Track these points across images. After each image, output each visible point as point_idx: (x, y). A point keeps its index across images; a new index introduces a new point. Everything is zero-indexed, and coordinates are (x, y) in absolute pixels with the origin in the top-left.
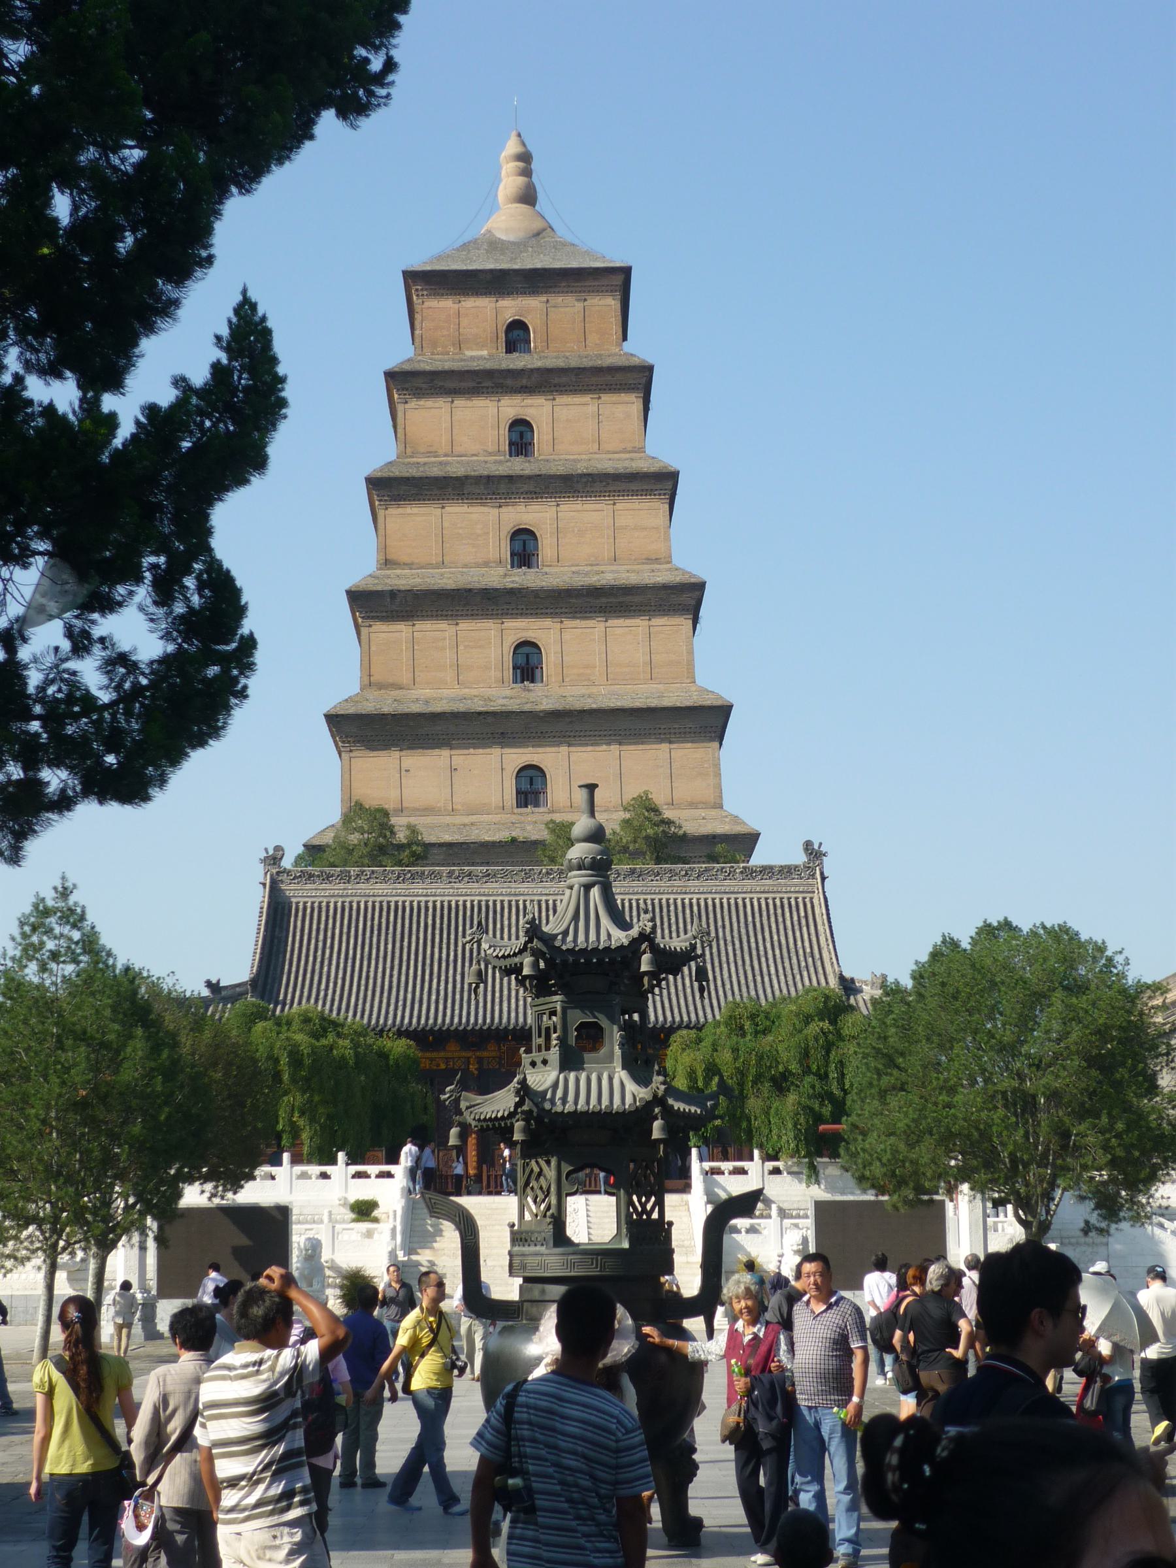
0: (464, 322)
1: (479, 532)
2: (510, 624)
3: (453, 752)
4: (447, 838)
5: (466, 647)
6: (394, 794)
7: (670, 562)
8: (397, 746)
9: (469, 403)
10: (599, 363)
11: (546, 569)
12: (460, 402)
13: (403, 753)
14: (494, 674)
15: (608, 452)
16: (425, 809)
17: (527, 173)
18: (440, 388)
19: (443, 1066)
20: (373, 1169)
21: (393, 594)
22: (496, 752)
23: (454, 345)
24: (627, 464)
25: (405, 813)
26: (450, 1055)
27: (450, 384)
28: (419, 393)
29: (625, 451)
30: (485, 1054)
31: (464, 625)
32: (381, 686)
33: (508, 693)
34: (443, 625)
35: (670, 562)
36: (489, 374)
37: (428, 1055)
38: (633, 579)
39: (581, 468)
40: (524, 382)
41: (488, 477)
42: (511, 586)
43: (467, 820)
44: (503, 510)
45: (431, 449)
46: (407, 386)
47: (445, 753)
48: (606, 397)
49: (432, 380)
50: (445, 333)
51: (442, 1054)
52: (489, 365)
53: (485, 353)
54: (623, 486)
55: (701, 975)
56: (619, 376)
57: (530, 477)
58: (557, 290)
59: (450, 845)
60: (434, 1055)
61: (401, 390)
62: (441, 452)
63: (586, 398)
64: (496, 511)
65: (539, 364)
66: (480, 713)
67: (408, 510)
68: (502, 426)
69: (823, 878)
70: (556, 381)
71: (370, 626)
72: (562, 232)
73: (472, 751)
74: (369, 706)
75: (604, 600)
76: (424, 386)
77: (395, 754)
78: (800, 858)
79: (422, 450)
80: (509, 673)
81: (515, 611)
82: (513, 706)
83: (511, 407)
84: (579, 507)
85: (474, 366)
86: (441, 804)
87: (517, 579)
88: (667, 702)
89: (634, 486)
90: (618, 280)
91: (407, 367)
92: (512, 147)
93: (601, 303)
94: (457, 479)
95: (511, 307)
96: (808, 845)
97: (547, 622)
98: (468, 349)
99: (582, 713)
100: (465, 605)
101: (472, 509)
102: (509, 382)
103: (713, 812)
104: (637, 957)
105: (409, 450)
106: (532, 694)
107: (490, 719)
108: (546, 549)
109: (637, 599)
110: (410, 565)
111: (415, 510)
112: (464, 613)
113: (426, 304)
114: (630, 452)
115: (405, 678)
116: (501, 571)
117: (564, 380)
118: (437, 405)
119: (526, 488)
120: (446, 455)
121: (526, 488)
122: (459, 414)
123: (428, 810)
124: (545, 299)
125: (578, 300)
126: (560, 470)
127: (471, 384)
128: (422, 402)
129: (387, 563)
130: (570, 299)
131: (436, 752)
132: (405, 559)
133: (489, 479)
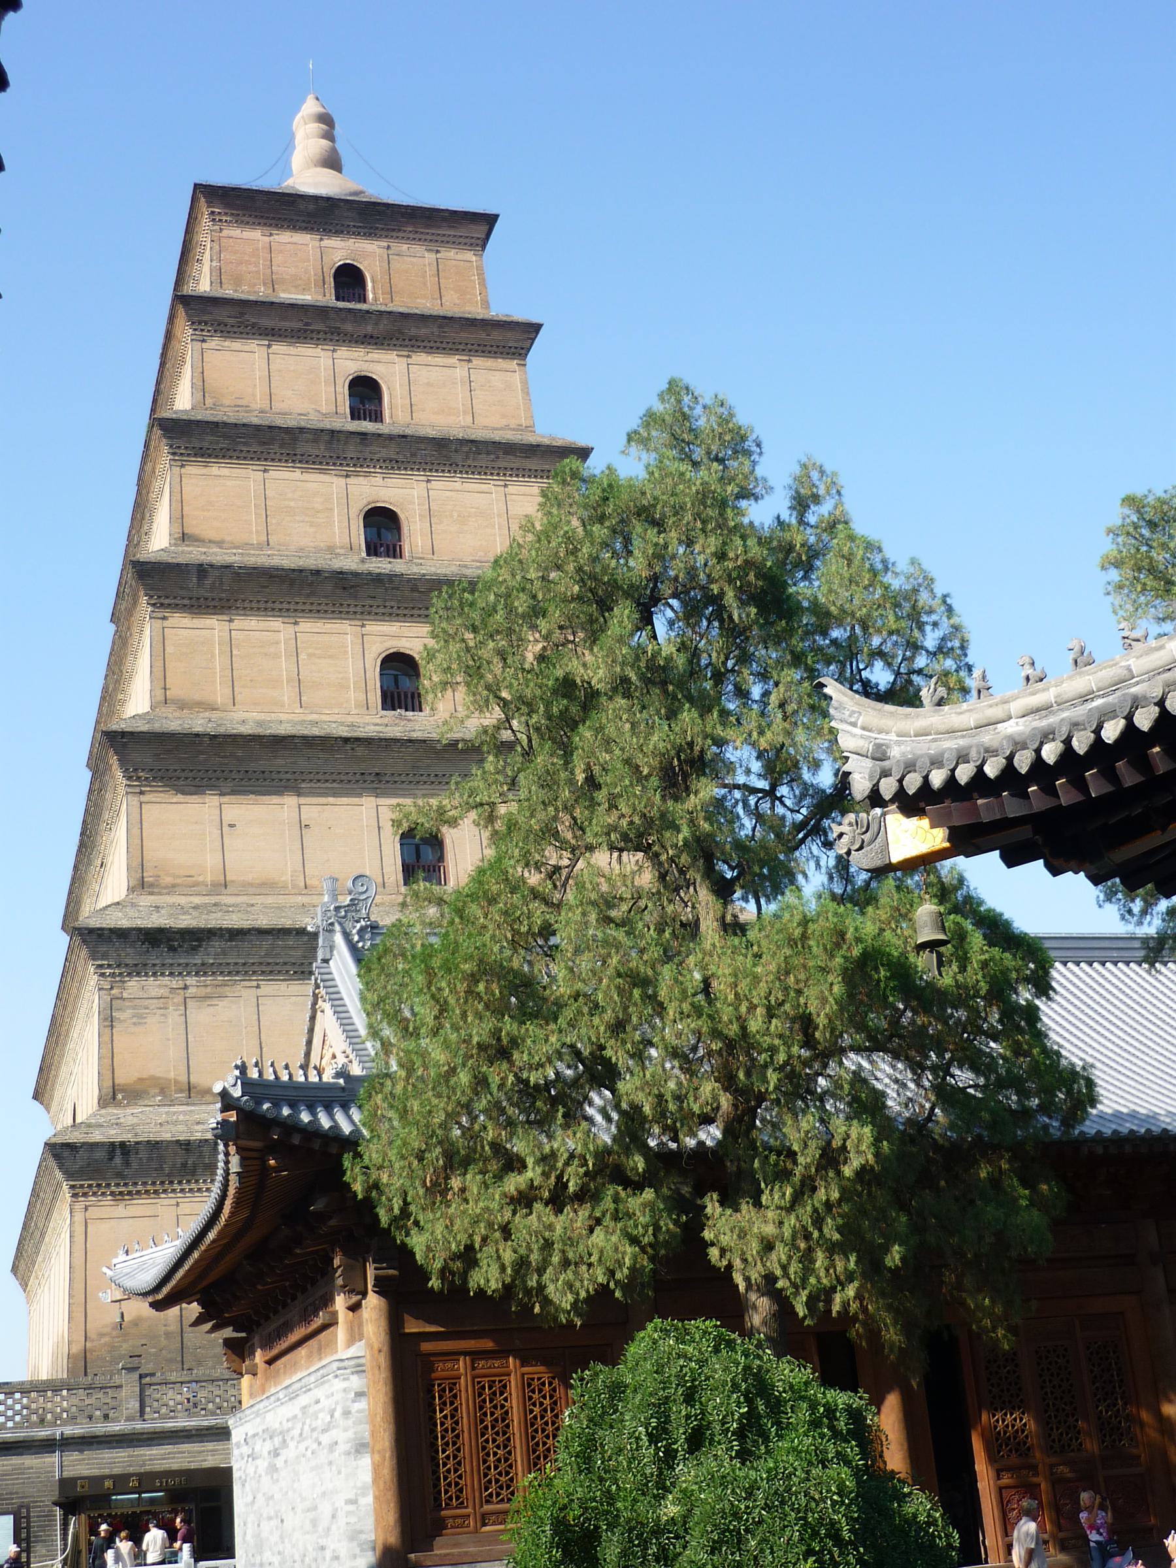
0: (278, 259)
2: (375, 628)
3: (303, 800)
5: (310, 656)
6: (211, 860)
8: (212, 787)
9: (292, 350)
12: (278, 348)
13: (225, 799)
14: (353, 696)
16: (263, 884)
17: (329, 136)
18: (253, 325)
21: (202, 570)
22: (368, 803)
23: (265, 284)
25: (230, 890)
27: (267, 322)
28: (225, 330)
31: (309, 627)
32: (182, 705)
34: (276, 623)
40: (369, 329)
41: (333, 432)
44: (351, 480)
45: (240, 402)
46: (205, 318)
47: (290, 801)
48: (477, 361)
49: (242, 314)
50: (252, 268)
54: (516, 462)
56: (496, 335)
58: (401, 234)
61: (196, 323)
63: (453, 360)
64: (342, 481)
66: (346, 740)
67: (215, 470)
68: (339, 382)
70: (413, 332)
71: (164, 618)
73: (331, 800)
76: (231, 321)
77: (212, 801)
79: (227, 402)
80: (376, 697)
81: (381, 610)
84: (458, 485)
86: (287, 878)
89: (533, 464)
92: (310, 107)
93: (459, 257)
94: (288, 430)
95: (342, 249)
98: (284, 291)
100: (308, 596)
101: (306, 476)
102: (349, 327)
105: (209, 401)
106: (410, 725)
107: (360, 751)
108: (414, 536)
111: (225, 472)
112: (307, 607)
113: (225, 233)
115: (220, 695)
117: (423, 331)
118: (246, 348)
119: (384, 453)
121: (384, 453)
122: (278, 363)
123: (267, 886)
124: (386, 244)
125: (428, 250)
127: (300, 325)
129: (184, 537)
130: (418, 249)
131: (275, 799)
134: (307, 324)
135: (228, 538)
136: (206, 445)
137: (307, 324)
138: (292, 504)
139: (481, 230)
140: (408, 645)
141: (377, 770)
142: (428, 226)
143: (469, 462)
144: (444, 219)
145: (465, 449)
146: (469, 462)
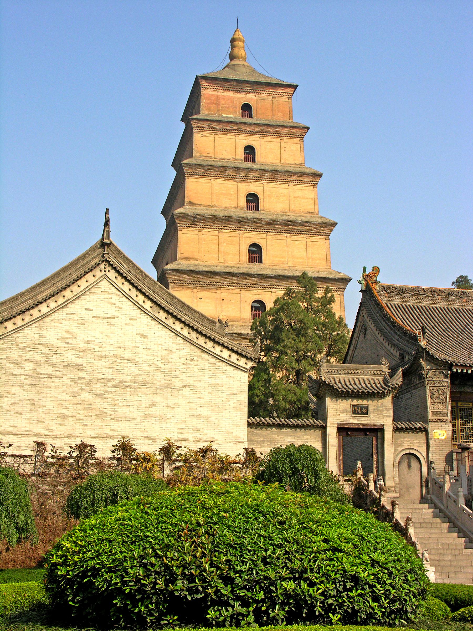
1: (232, 193)
9: (227, 137)
18: (214, 128)
24: (299, 169)
27: (218, 127)
35: (317, 214)
39: (279, 168)
48: (286, 140)
53: (232, 116)
54: (296, 178)
56: (293, 130)
57: (257, 170)
62: (213, 156)
65: (258, 122)
75: (291, 227)
76: (207, 126)
79: (205, 155)
82: (252, 271)
88: (321, 276)
89: (302, 179)
94: (223, 167)
97: (263, 235)
98: (224, 114)
109: (306, 228)
114: (298, 165)
117: (270, 130)
120: (215, 158)
126: (269, 168)
127: (229, 128)
128: (206, 134)
133: (238, 169)
134: (232, 128)
135: (203, 203)
136: (197, 171)
137: (232, 128)
138: (224, 192)
139: (291, 90)
140: (258, 241)
141: (246, 283)
142: (274, 89)
143: (281, 178)
144: (280, 87)
145: (280, 174)
146: (281, 178)
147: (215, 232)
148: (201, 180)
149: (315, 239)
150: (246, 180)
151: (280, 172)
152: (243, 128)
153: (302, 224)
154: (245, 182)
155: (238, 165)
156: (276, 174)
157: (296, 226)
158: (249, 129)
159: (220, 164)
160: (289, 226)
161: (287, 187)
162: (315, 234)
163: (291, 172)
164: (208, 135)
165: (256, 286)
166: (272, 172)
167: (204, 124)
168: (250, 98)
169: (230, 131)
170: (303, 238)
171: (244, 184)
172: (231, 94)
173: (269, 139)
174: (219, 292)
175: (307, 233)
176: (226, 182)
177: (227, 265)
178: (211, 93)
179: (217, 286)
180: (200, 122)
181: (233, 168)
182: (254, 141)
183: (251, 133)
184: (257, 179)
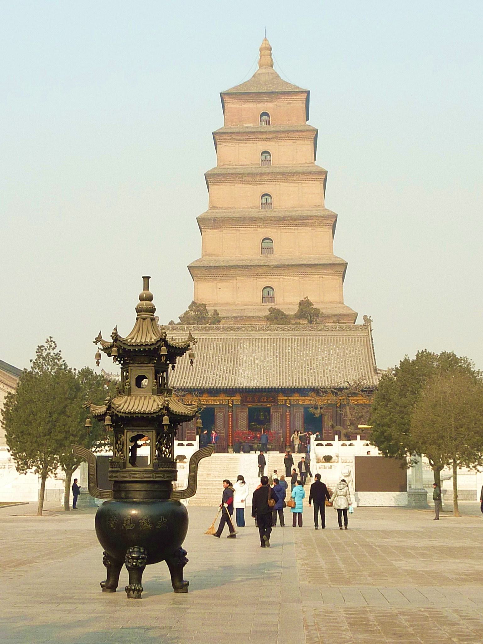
2: (261, 230)
4: (235, 315)
7: (323, 207)
10: (296, 129)
11: (275, 210)
12: (242, 144)
15: (300, 164)
19: (218, 403)
20: (186, 443)
21: (215, 220)
24: (307, 168)
26: (221, 398)
27: (237, 137)
29: (306, 163)
30: (235, 398)
32: (209, 255)
33: (259, 258)
36: (253, 133)
37: (212, 398)
38: (309, 213)
39: (289, 170)
42: (260, 216)
43: (242, 308)
48: (299, 142)
51: (218, 398)
52: (253, 130)
53: (252, 125)
55: (192, 356)
57: (269, 174)
59: (236, 317)
60: (215, 398)
65: (273, 129)
69: (371, 330)
72: (282, 77)
74: (205, 263)
75: (297, 222)
78: (363, 322)
82: (262, 263)
83: (261, 146)
85: (247, 130)
87: (263, 213)
89: (310, 177)
90: (305, 96)
91: (222, 131)
94: (240, 174)
95: (262, 107)
96: (365, 316)
97: (275, 230)
98: (245, 124)
99: (288, 266)
103: (340, 305)
104: (159, 347)
108: (276, 201)
109: (310, 221)
110: (221, 208)
116: (257, 210)
117: (283, 135)
119: (267, 178)
121: (267, 178)
123: (227, 304)
126: (281, 170)
129: (212, 207)
132: (218, 206)
133: (253, 175)
147: (233, 231)
148: (222, 186)
149: (319, 229)
150: (260, 183)
151: (289, 173)
152: (260, 136)
153: (307, 218)
154: (260, 184)
155: (254, 171)
156: (286, 175)
157: (301, 220)
158: (264, 136)
159: (238, 171)
160: (295, 220)
161: (296, 185)
162: (319, 225)
163: (299, 173)
164: (229, 145)
165: (266, 274)
166: (283, 174)
167: (225, 136)
168: (268, 106)
169: (248, 140)
170: (309, 229)
171: (258, 186)
172: (251, 105)
173: (283, 143)
174: (235, 281)
175: (312, 225)
176: (244, 186)
177: (243, 258)
178: (233, 106)
179: (234, 277)
180: (222, 135)
181: (248, 174)
182: (270, 146)
183: (267, 139)
184: (270, 181)
